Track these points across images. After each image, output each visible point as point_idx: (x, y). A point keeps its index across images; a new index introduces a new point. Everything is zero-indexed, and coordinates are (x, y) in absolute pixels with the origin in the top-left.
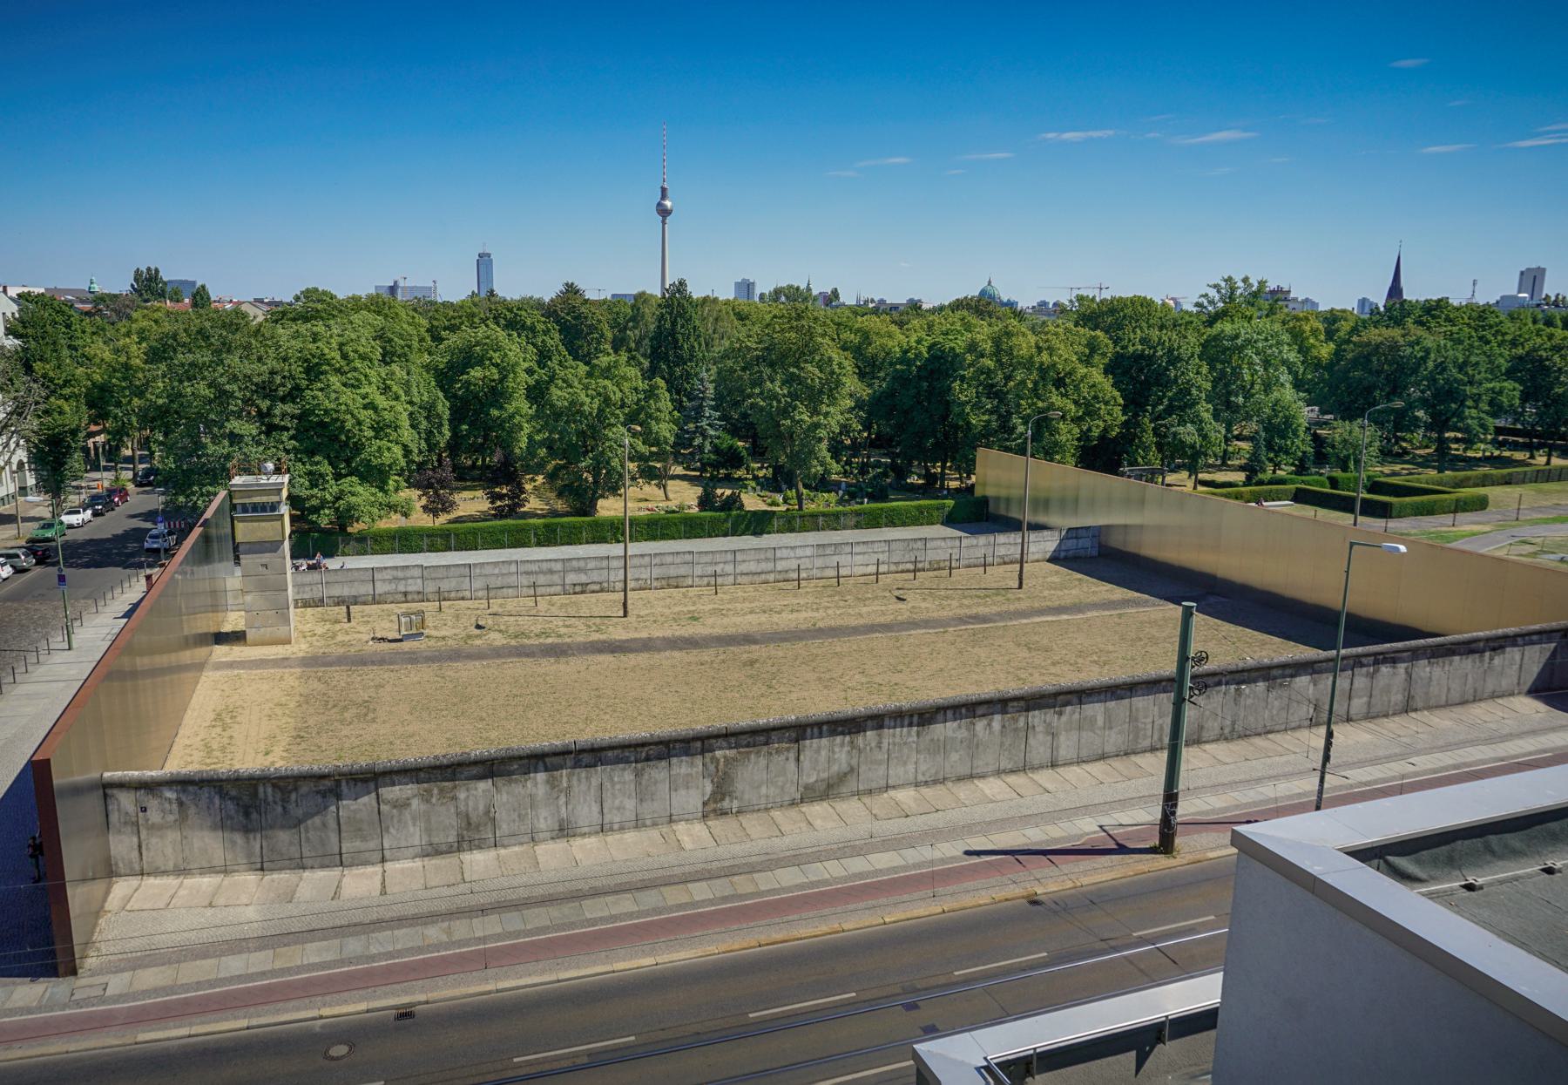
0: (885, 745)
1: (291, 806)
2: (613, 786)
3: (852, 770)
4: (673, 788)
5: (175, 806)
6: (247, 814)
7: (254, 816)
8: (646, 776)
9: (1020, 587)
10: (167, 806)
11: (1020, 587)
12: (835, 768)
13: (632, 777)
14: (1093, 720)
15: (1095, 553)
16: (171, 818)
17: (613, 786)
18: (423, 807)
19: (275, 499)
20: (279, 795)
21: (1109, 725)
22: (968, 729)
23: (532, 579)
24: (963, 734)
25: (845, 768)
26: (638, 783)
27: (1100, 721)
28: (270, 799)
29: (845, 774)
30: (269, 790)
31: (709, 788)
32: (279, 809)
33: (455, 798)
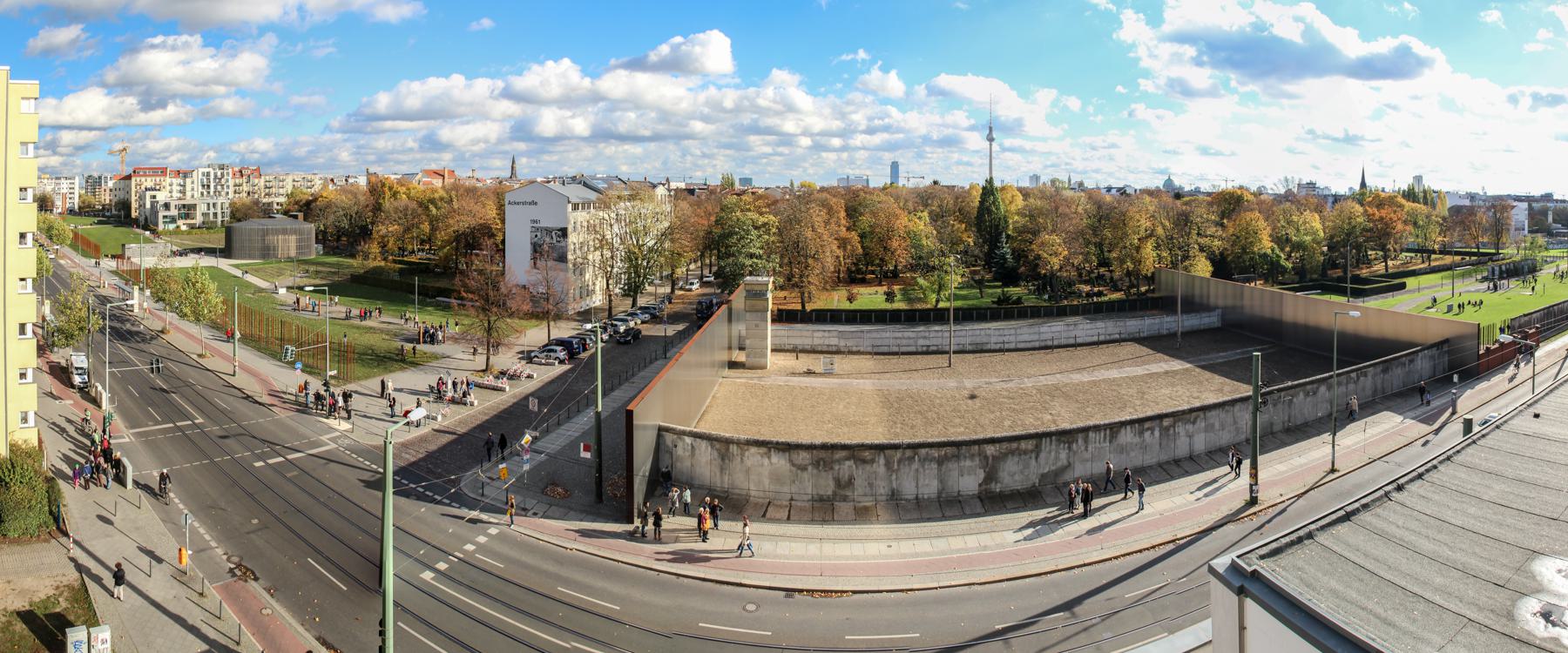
26: (939, 470)
31: (981, 475)
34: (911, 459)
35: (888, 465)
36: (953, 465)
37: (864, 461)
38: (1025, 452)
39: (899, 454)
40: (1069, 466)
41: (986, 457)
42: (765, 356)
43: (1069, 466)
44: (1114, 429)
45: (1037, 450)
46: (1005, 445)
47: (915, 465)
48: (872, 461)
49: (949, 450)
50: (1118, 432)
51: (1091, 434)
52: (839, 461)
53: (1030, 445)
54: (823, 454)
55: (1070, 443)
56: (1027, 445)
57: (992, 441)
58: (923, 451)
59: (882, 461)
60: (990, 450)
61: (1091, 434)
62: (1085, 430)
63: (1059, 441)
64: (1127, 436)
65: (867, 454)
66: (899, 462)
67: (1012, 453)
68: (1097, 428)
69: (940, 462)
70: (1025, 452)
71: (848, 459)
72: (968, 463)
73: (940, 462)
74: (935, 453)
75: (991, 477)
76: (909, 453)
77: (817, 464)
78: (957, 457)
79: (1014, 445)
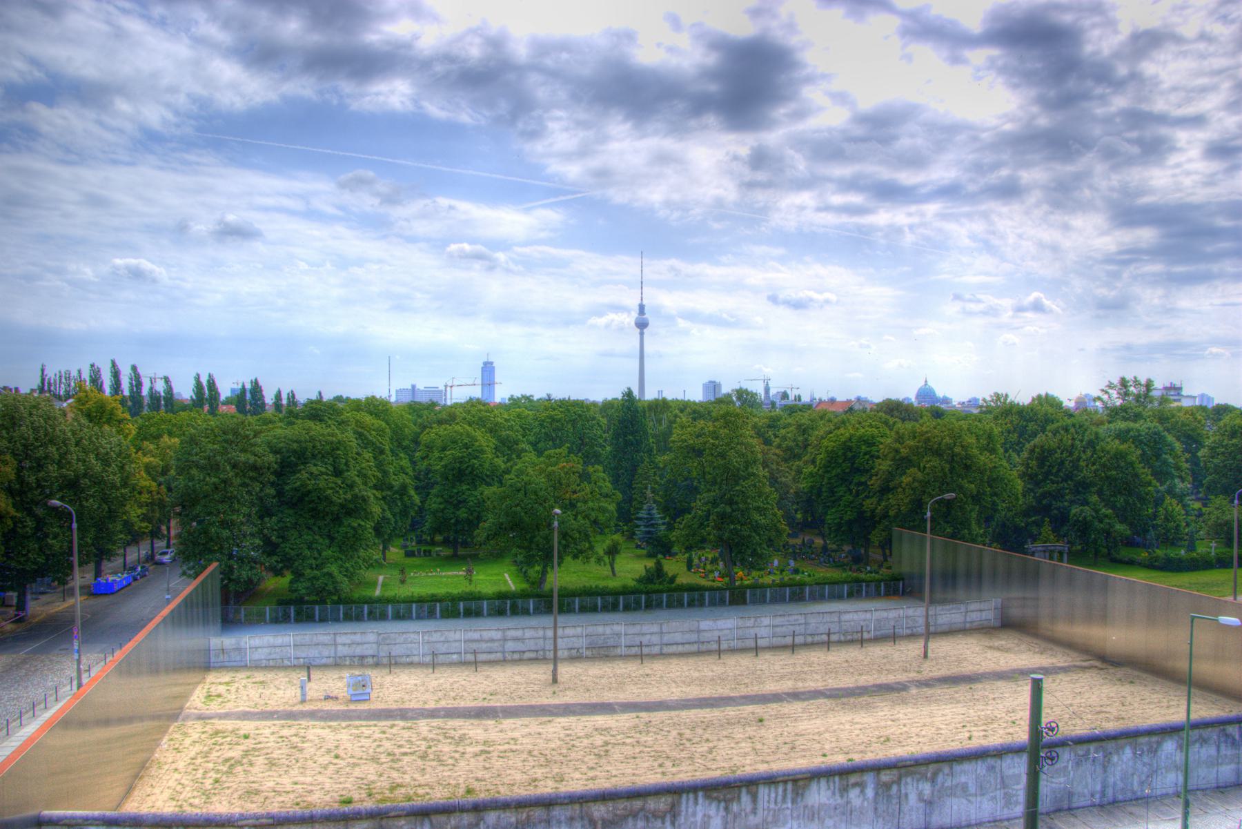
0: (760, 812)
14: (964, 788)
15: (998, 624)
21: (982, 790)
22: (842, 797)
23: (474, 646)
38: (656, 815)
44: (799, 782)
45: (674, 812)
46: (622, 805)
50: (805, 787)
51: (763, 792)
53: (662, 803)
56: (652, 804)
60: (599, 811)
61: (763, 792)
62: (751, 784)
63: (707, 797)
67: (635, 815)
68: (771, 780)
70: (656, 815)
79: (638, 804)
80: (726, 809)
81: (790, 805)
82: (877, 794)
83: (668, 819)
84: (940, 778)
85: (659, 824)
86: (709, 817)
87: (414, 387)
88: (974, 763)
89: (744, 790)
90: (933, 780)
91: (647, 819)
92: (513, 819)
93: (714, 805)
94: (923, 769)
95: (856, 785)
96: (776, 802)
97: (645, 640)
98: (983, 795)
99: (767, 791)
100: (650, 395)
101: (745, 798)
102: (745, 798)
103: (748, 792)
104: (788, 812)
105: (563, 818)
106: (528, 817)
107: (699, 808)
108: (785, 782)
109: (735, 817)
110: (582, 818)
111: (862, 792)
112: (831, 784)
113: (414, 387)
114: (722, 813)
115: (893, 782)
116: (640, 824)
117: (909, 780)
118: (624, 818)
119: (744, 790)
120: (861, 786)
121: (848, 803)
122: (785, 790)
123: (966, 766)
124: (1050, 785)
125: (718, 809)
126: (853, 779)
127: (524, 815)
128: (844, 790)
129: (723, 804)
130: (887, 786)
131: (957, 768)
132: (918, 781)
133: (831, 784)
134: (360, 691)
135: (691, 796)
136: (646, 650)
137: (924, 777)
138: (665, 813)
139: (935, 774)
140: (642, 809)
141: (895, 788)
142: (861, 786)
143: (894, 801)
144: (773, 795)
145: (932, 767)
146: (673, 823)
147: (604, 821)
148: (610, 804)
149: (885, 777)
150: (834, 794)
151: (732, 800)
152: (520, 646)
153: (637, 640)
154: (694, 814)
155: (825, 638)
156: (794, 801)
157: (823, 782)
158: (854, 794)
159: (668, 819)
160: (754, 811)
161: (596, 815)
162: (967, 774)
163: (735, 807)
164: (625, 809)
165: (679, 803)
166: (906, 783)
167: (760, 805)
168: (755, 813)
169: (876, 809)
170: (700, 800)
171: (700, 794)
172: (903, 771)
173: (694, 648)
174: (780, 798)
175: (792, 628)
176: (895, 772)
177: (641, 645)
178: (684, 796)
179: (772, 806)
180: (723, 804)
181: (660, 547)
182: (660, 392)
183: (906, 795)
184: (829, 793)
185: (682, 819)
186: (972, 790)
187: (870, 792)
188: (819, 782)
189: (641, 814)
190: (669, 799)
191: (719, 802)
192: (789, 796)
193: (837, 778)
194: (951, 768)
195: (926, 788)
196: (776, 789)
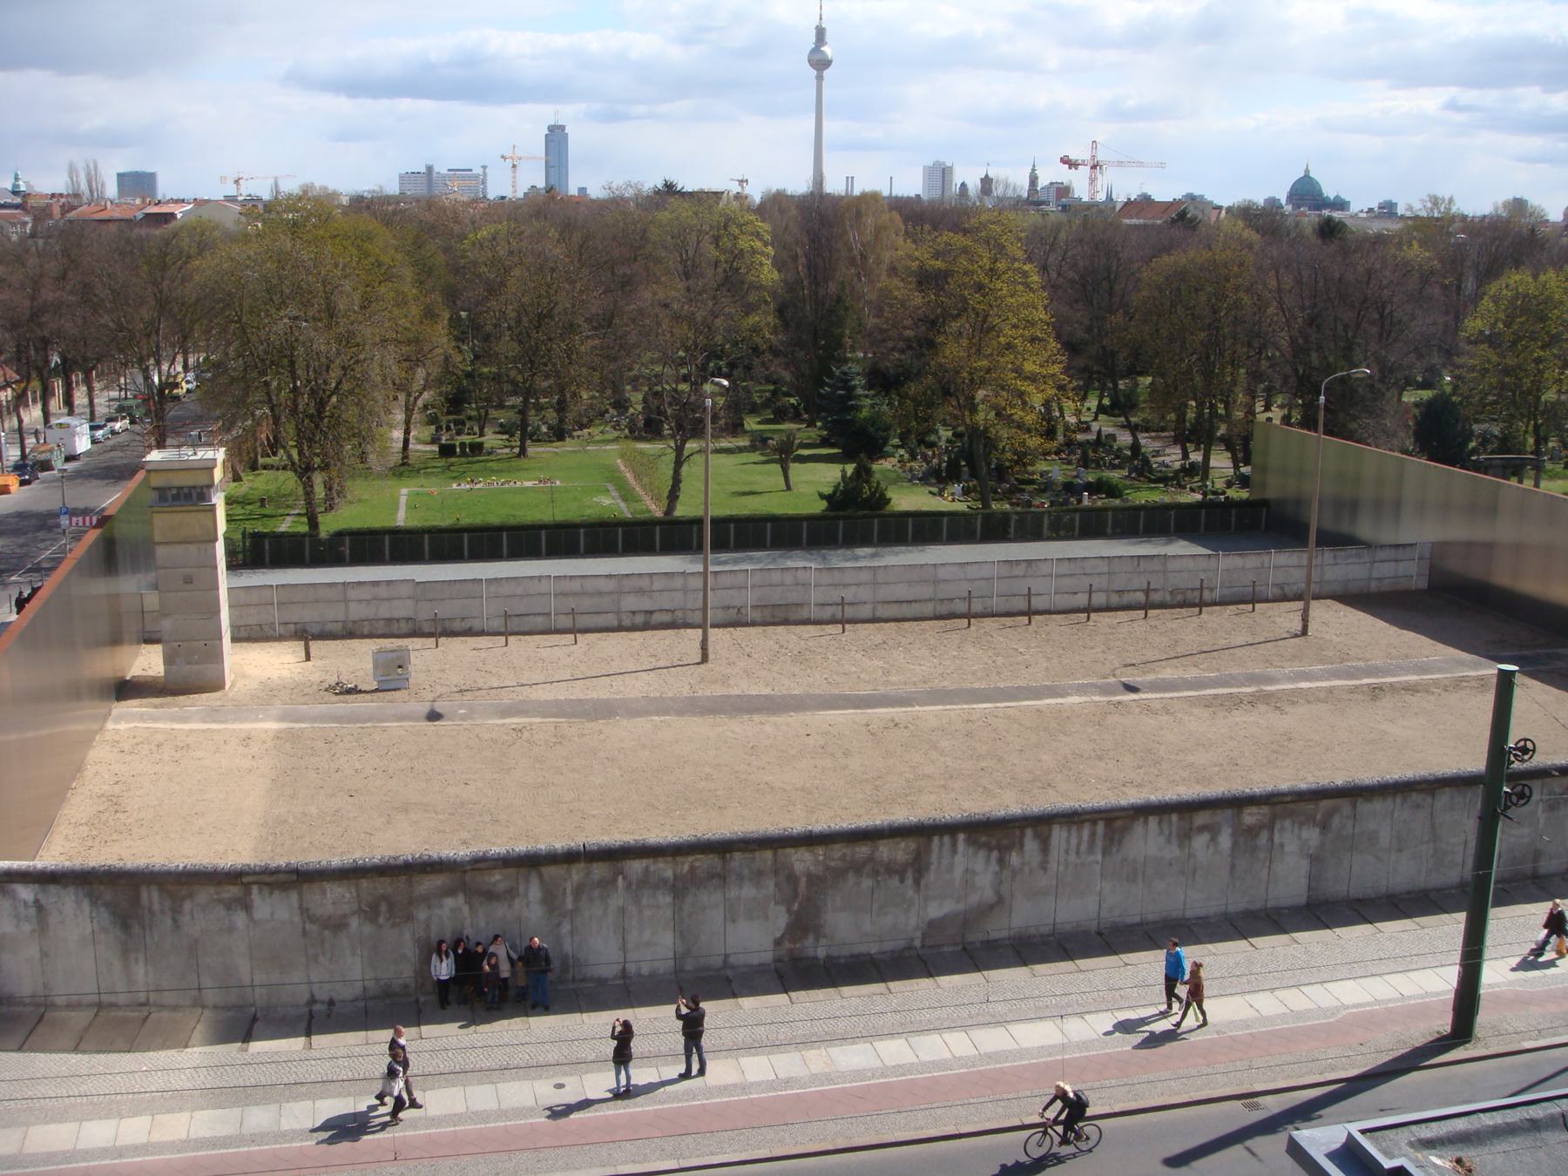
0: (1053, 866)
1: (185, 919)
2: (640, 912)
3: (1000, 900)
4: (731, 916)
5: (33, 911)
6: (126, 927)
7: (136, 930)
8: (689, 899)
9: (705, 658)
10: (22, 909)
11: (705, 658)
12: (974, 899)
13: (669, 899)
16: (26, 928)
17: (640, 912)
18: (368, 929)
19: (201, 480)
20: (168, 903)
22: (1181, 846)
24: (1172, 852)
25: (989, 895)
27: (1385, 837)
28: (156, 907)
29: (991, 907)
30: (155, 895)
32: (169, 922)
33: (409, 918)
34: (608, 884)
35: (550, 900)
36: (710, 901)
37: (491, 896)
38: (891, 869)
39: (577, 873)
40: (999, 902)
41: (792, 878)
42: (217, 657)
43: (999, 902)
44: (1114, 823)
45: (919, 865)
46: (838, 851)
47: (618, 899)
48: (511, 894)
49: (704, 862)
50: (1125, 830)
51: (1058, 834)
52: (426, 900)
53: (899, 851)
54: (384, 886)
55: (1004, 850)
56: (885, 850)
57: (809, 840)
58: (636, 866)
59: (535, 892)
60: (802, 861)
61: (1058, 834)
62: (1041, 823)
63: (970, 842)
64: (1147, 841)
65: (497, 878)
66: (579, 890)
67: (857, 868)
68: (1072, 818)
69: (679, 889)
70: (891, 869)
71: (450, 892)
72: (748, 891)
73: (679, 889)
74: (665, 869)
75: (804, 923)
76: (600, 870)
77: (370, 912)
78: (722, 878)
79: (863, 850)
80: (1001, 861)
81: (1099, 857)
82: (1235, 844)
83: (909, 875)
84: (1336, 821)
85: (894, 881)
86: (974, 873)
87: (430, 169)
88: (1389, 801)
89: (1029, 832)
90: (1324, 826)
91: (876, 873)
92: (669, 874)
93: (982, 853)
94: (1309, 807)
95: (1204, 828)
96: (1078, 853)
97: (848, 594)
98: (1400, 850)
99: (1064, 834)
100: (857, 192)
101: (1031, 844)
102: (1031, 844)
103: (1036, 836)
104: (1098, 868)
105: (746, 872)
106: (692, 868)
107: (959, 858)
108: (1094, 822)
109: (1014, 873)
110: (776, 873)
111: (1213, 839)
112: (1165, 827)
113: (430, 169)
114: (994, 867)
115: (1262, 827)
116: (867, 883)
117: (1287, 823)
118: (839, 874)
119: (1029, 832)
120: (1212, 830)
121: (1190, 855)
122: (1093, 834)
123: (1377, 805)
124: (1507, 838)
125: (988, 858)
126: (1201, 818)
127: (686, 867)
128: (1185, 836)
129: (995, 854)
130: (1252, 832)
131: (1364, 807)
132: (1301, 825)
133: (1165, 827)
134: (392, 677)
135: (946, 839)
136: (850, 612)
137: (1310, 820)
138: (905, 866)
139: (1329, 815)
140: (870, 859)
141: (1264, 835)
142: (1212, 830)
143: (1262, 855)
144: (1074, 841)
145: (1325, 804)
146: (917, 882)
147: (809, 876)
148: (820, 851)
149: (1250, 816)
150: (1169, 841)
151: (1009, 848)
152: (647, 604)
153: (835, 595)
154: (951, 868)
155: (1140, 597)
156: (1106, 852)
157: (1153, 821)
158: (1200, 841)
159: (909, 875)
160: (1044, 866)
161: (798, 867)
162: (1378, 818)
163: (1014, 859)
164: (844, 856)
165: (928, 850)
166: (1282, 829)
167: (1054, 855)
168: (1045, 869)
169: (1233, 867)
170: (961, 846)
171: (961, 837)
172: (1279, 808)
173: (928, 609)
174: (1084, 846)
175: (1086, 581)
176: (1265, 810)
177: (842, 603)
178: (936, 839)
179: (1072, 858)
180: (995, 854)
181: (858, 443)
182: (850, 180)
183: (1282, 846)
184: (1162, 839)
185: (931, 877)
186: (1385, 837)
187: (1225, 841)
188: (1146, 822)
189: (868, 867)
190: (912, 844)
191: (990, 849)
192: (1099, 843)
193: (1174, 817)
194: (1354, 807)
195: (1312, 835)
196: (1079, 831)
